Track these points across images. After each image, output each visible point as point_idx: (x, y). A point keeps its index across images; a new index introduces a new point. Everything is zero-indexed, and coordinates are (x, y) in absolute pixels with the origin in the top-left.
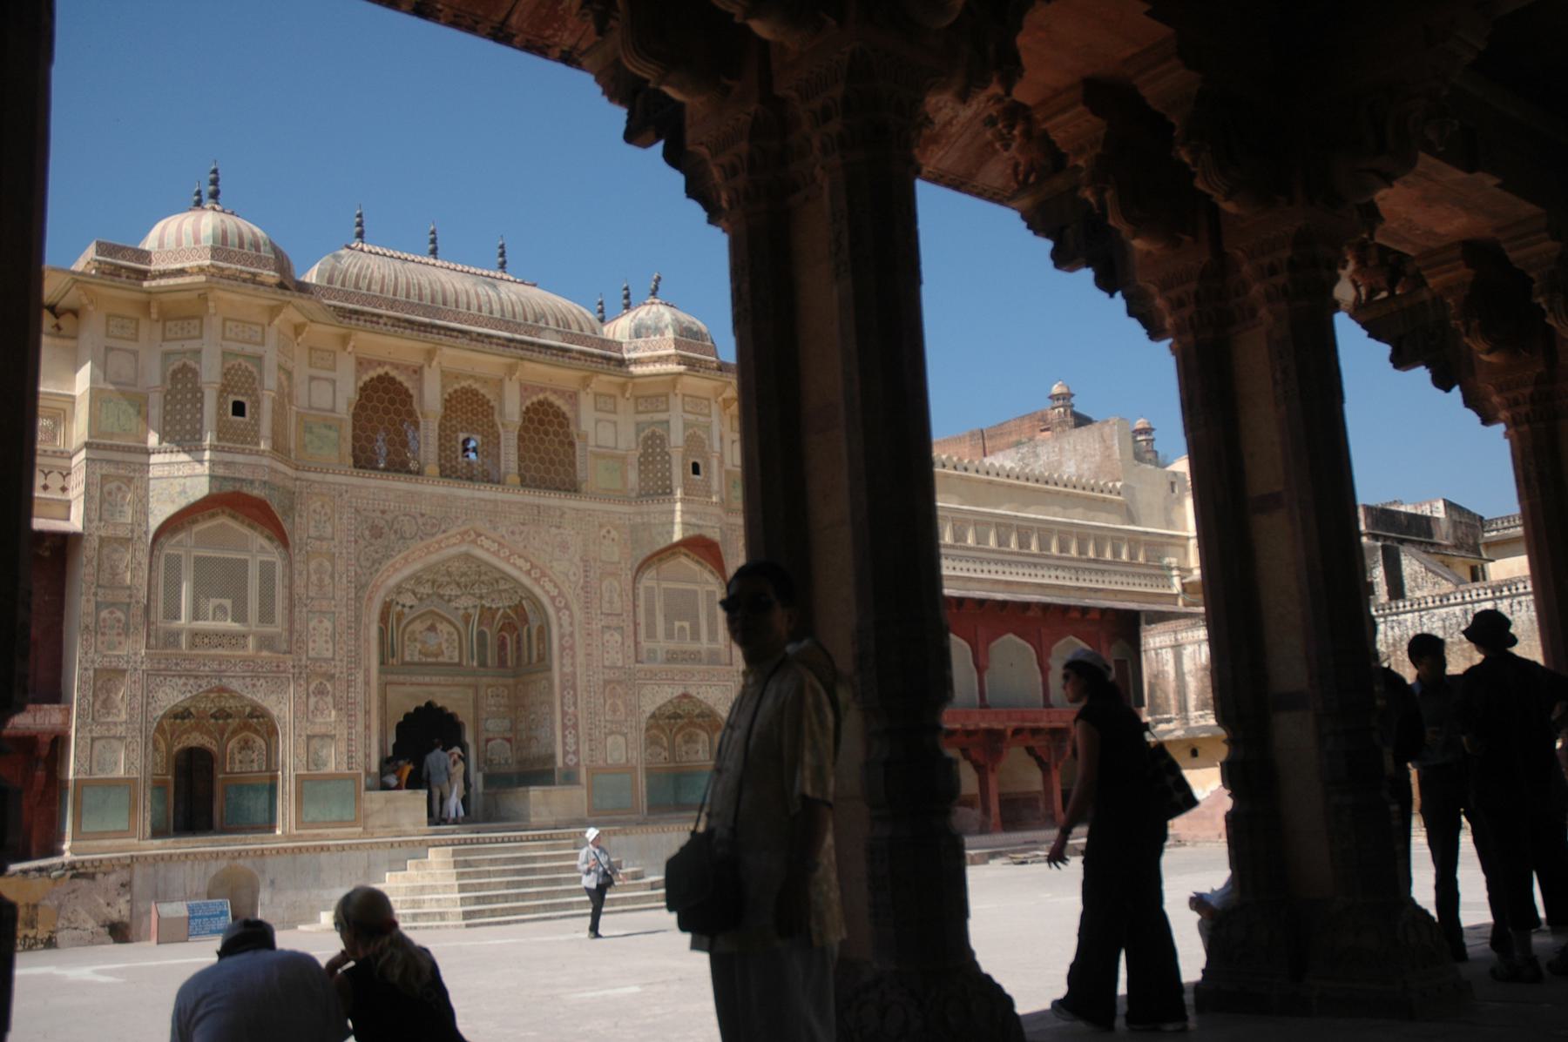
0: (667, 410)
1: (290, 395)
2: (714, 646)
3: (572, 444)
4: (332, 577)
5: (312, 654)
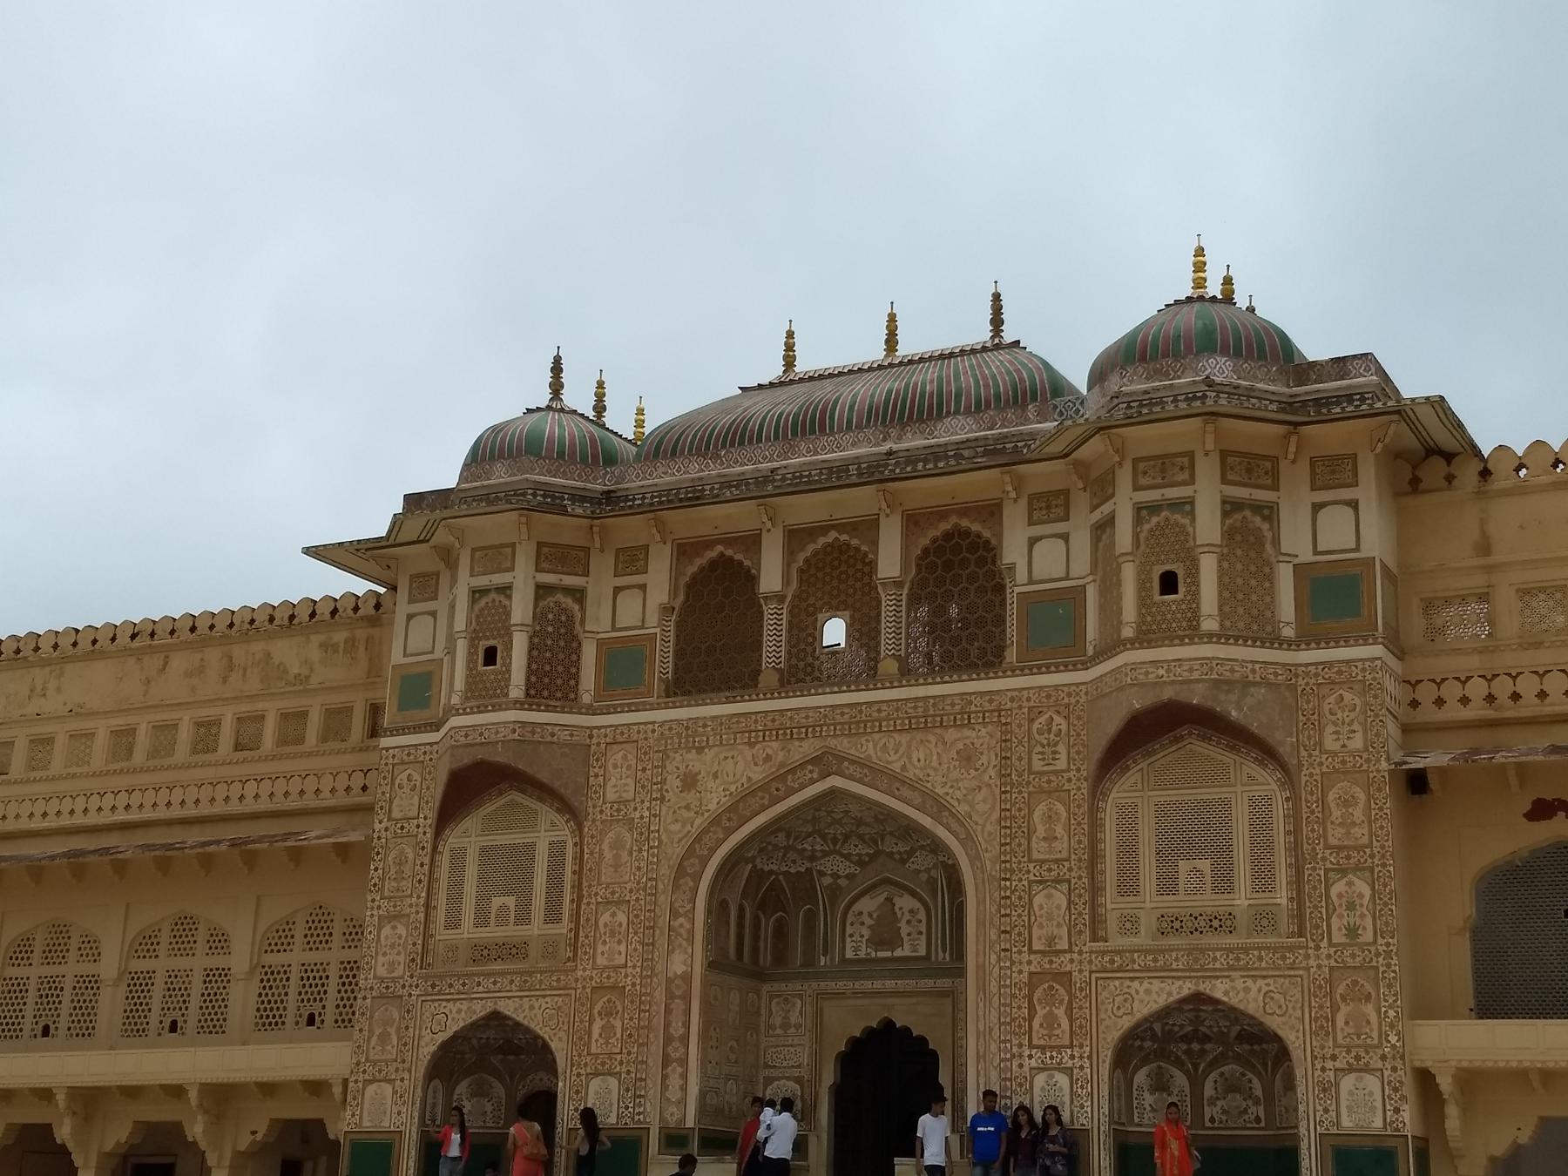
0: (1113, 495)
1: (583, 622)
2: (1263, 899)
3: (1000, 589)
4: (631, 854)
5: (601, 961)
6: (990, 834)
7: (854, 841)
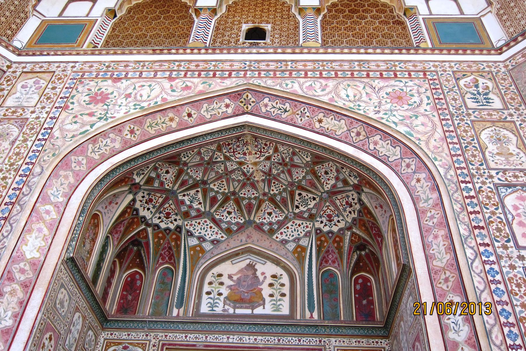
1: (35, 6)
3: (401, 23)
4: (13, 142)
6: (436, 148)
7: (231, 206)
